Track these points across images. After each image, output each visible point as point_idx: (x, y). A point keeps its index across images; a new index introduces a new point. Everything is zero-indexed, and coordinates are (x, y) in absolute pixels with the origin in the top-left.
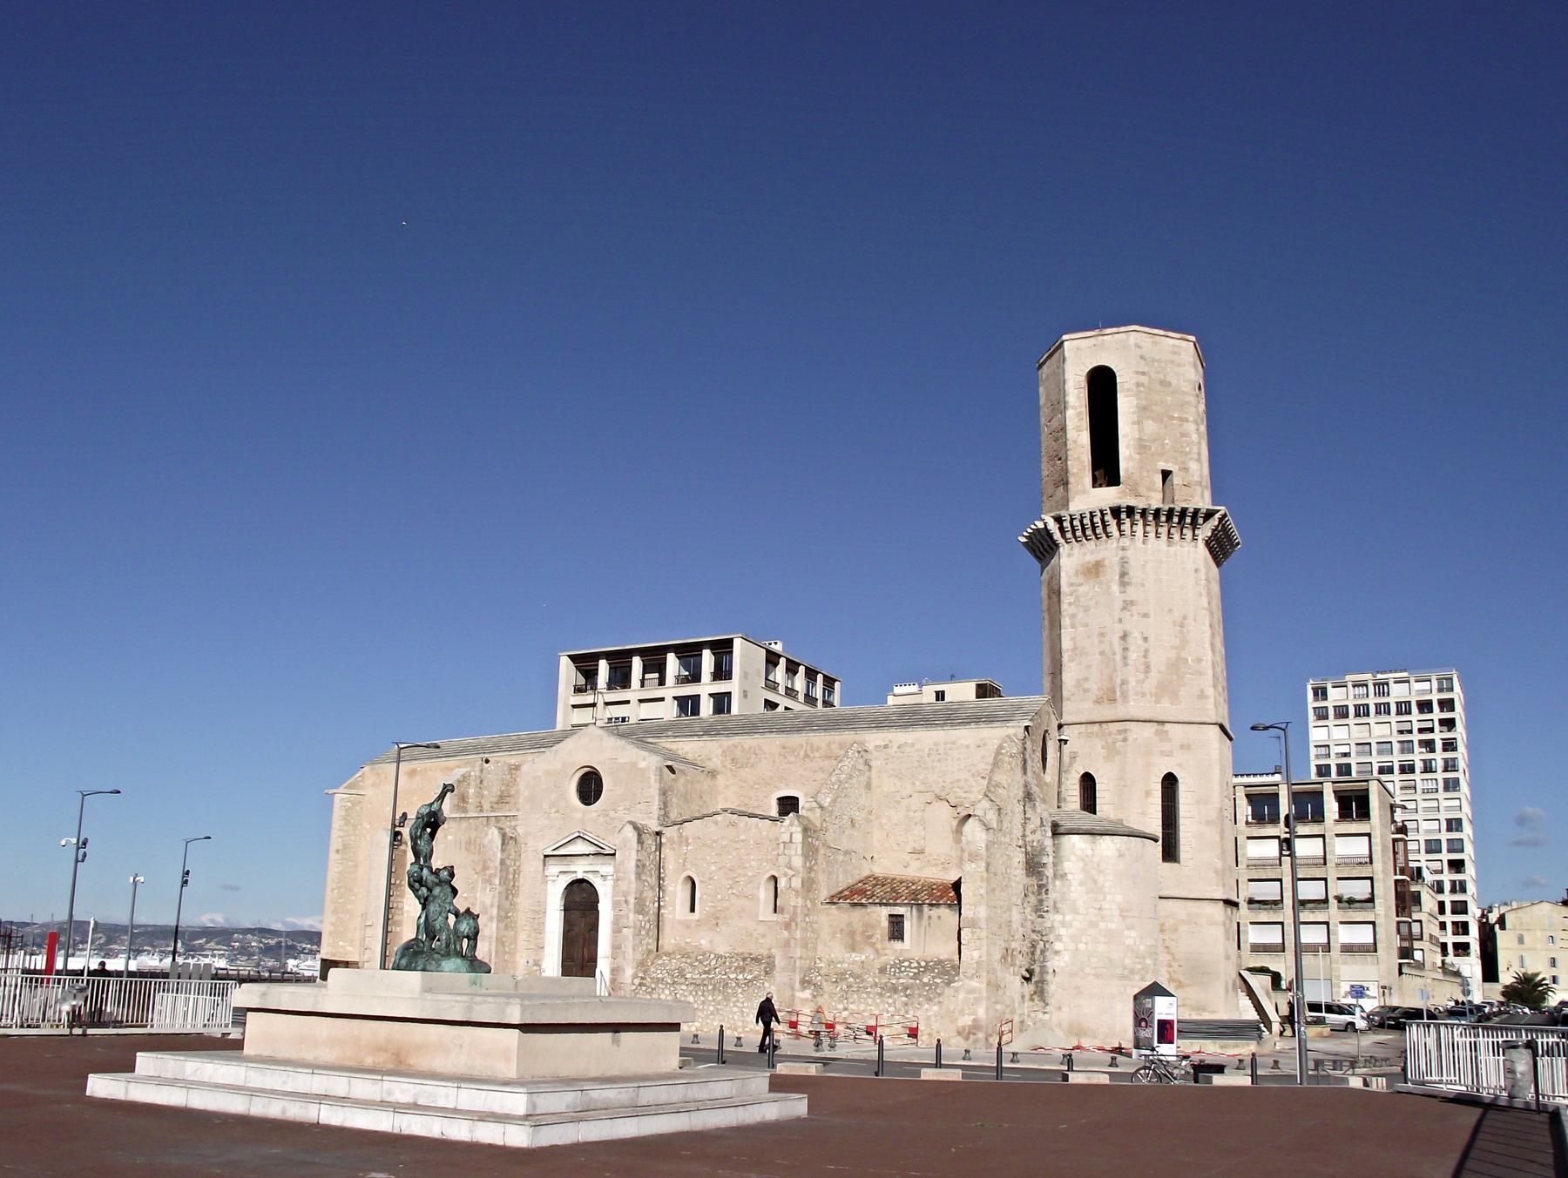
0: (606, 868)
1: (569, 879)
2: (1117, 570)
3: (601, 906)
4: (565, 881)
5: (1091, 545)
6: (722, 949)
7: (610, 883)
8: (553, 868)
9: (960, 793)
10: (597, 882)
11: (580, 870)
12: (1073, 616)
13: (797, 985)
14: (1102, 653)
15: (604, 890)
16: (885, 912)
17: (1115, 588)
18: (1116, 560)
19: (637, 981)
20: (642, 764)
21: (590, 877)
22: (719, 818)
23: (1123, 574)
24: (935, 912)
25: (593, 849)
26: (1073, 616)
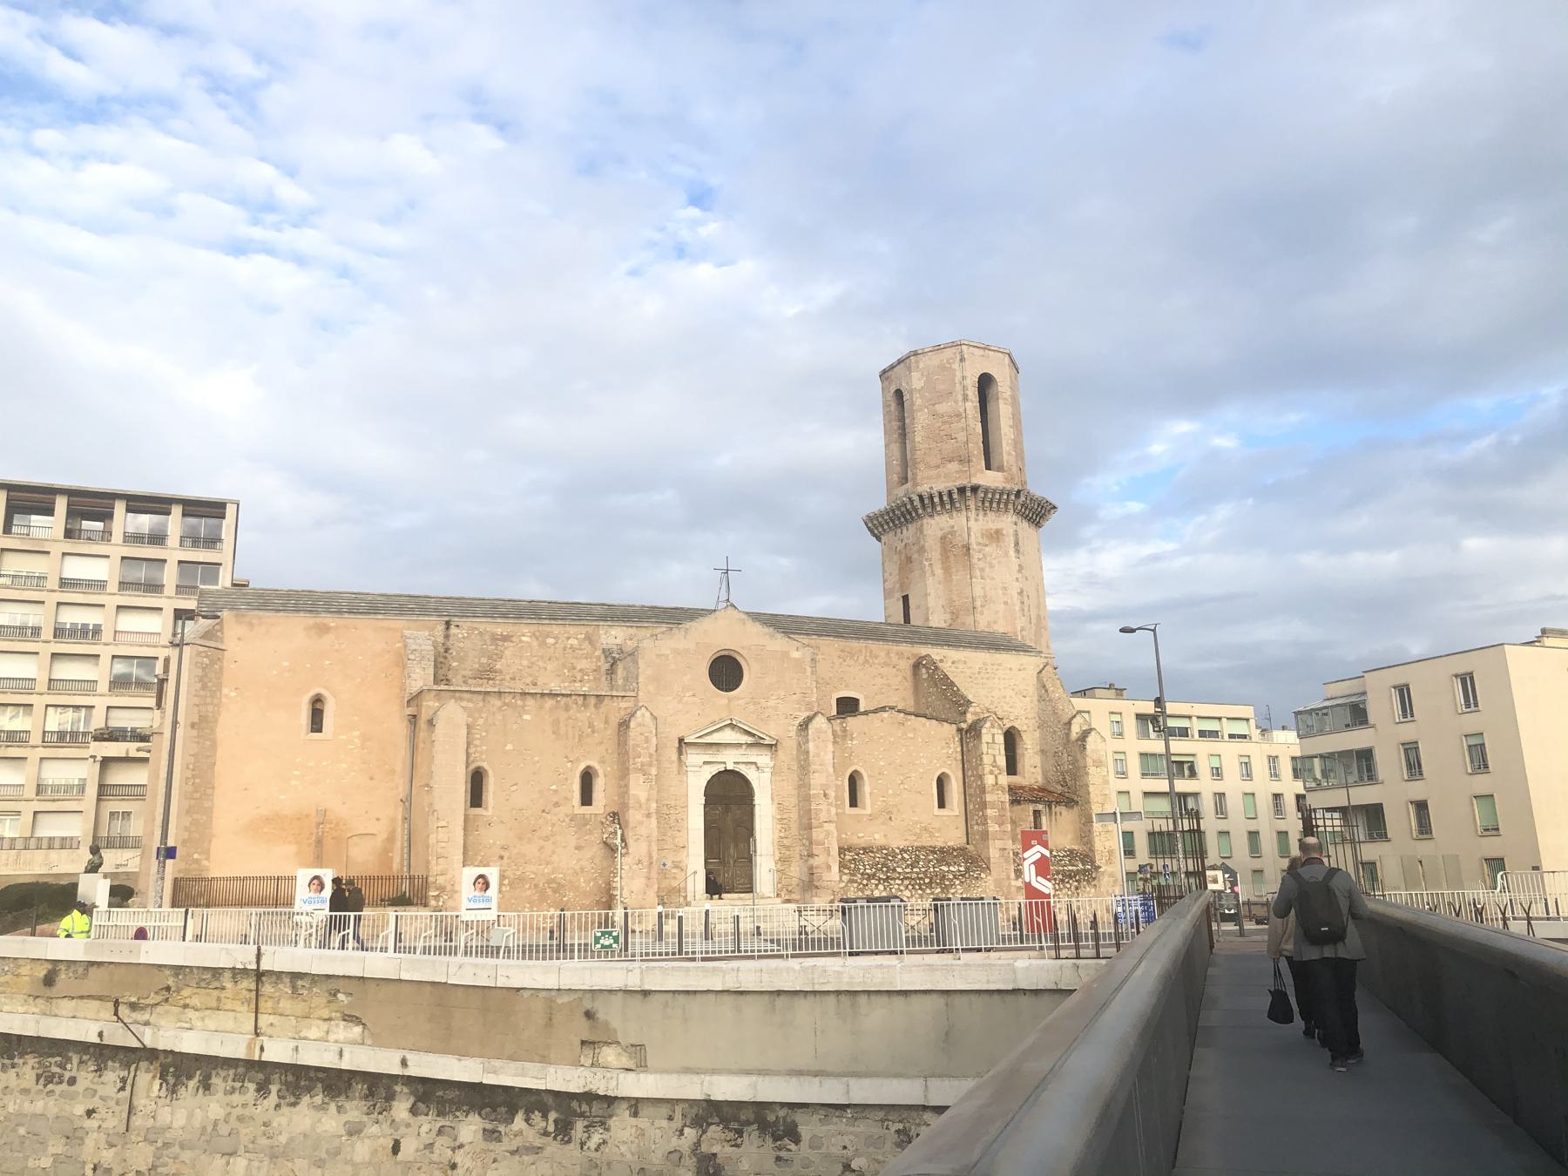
0: (764, 758)
1: (715, 769)
2: (1012, 538)
3: (757, 801)
4: (709, 772)
5: (991, 515)
6: (897, 842)
7: (767, 776)
8: (694, 758)
9: (1006, 708)
10: (750, 774)
11: (730, 760)
12: (982, 570)
13: (1013, 875)
14: (1006, 603)
15: (761, 783)
16: (1031, 807)
17: (1012, 553)
18: (1011, 531)
19: (845, 878)
20: (796, 655)
21: (743, 769)
22: (885, 715)
23: (1017, 544)
24: (1058, 809)
25: (750, 740)
26: (982, 570)
